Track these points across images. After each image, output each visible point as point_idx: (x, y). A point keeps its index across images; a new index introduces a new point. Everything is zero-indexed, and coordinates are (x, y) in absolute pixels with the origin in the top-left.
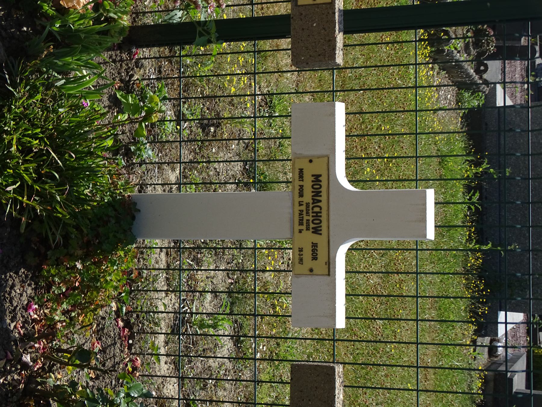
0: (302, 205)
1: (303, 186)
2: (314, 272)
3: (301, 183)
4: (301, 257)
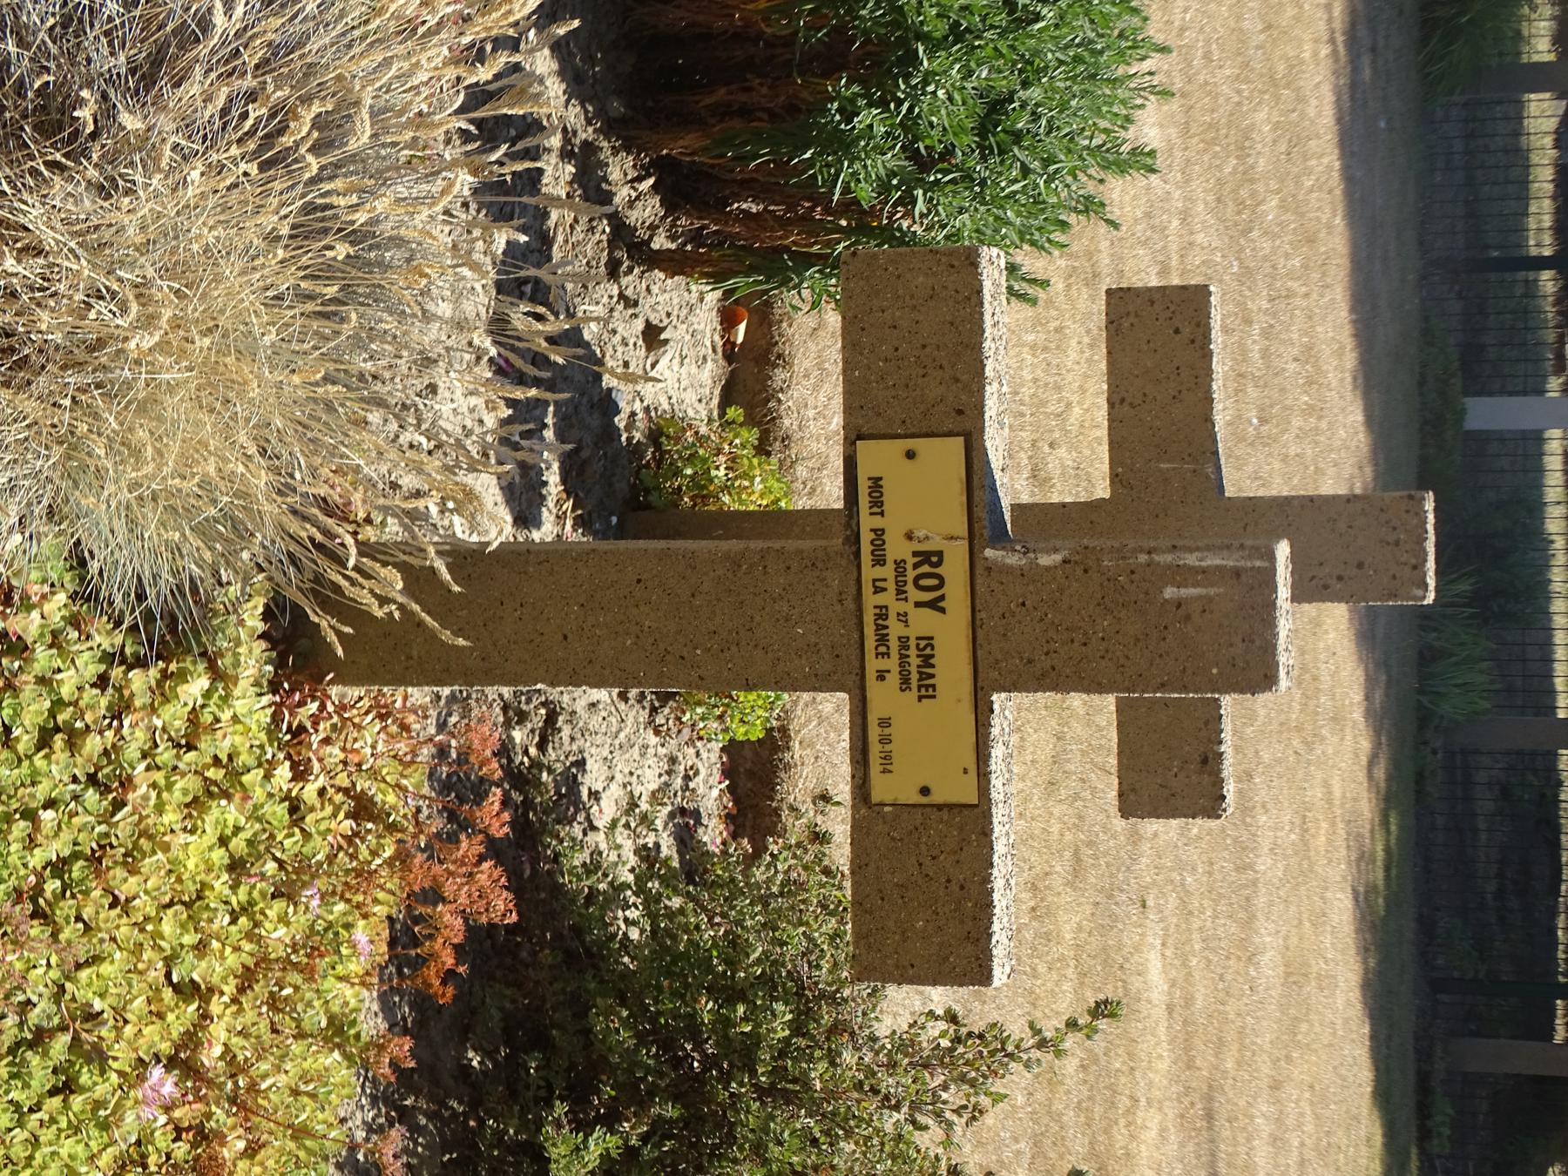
3: (877, 522)
4: (888, 747)
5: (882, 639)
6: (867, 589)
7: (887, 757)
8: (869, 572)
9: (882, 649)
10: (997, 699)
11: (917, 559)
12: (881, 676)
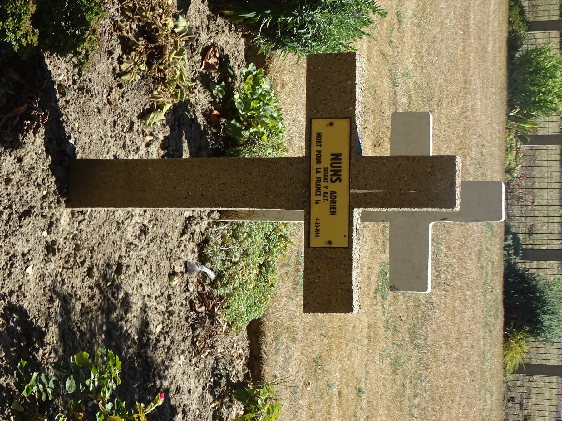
0: (320, 172)
1: (321, 151)
3: (319, 148)
4: (318, 228)
5: (318, 189)
6: (313, 172)
7: (318, 231)
8: (314, 165)
9: (318, 193)
10: (357, 212)
11: (333, 157)
12: (317, 202)
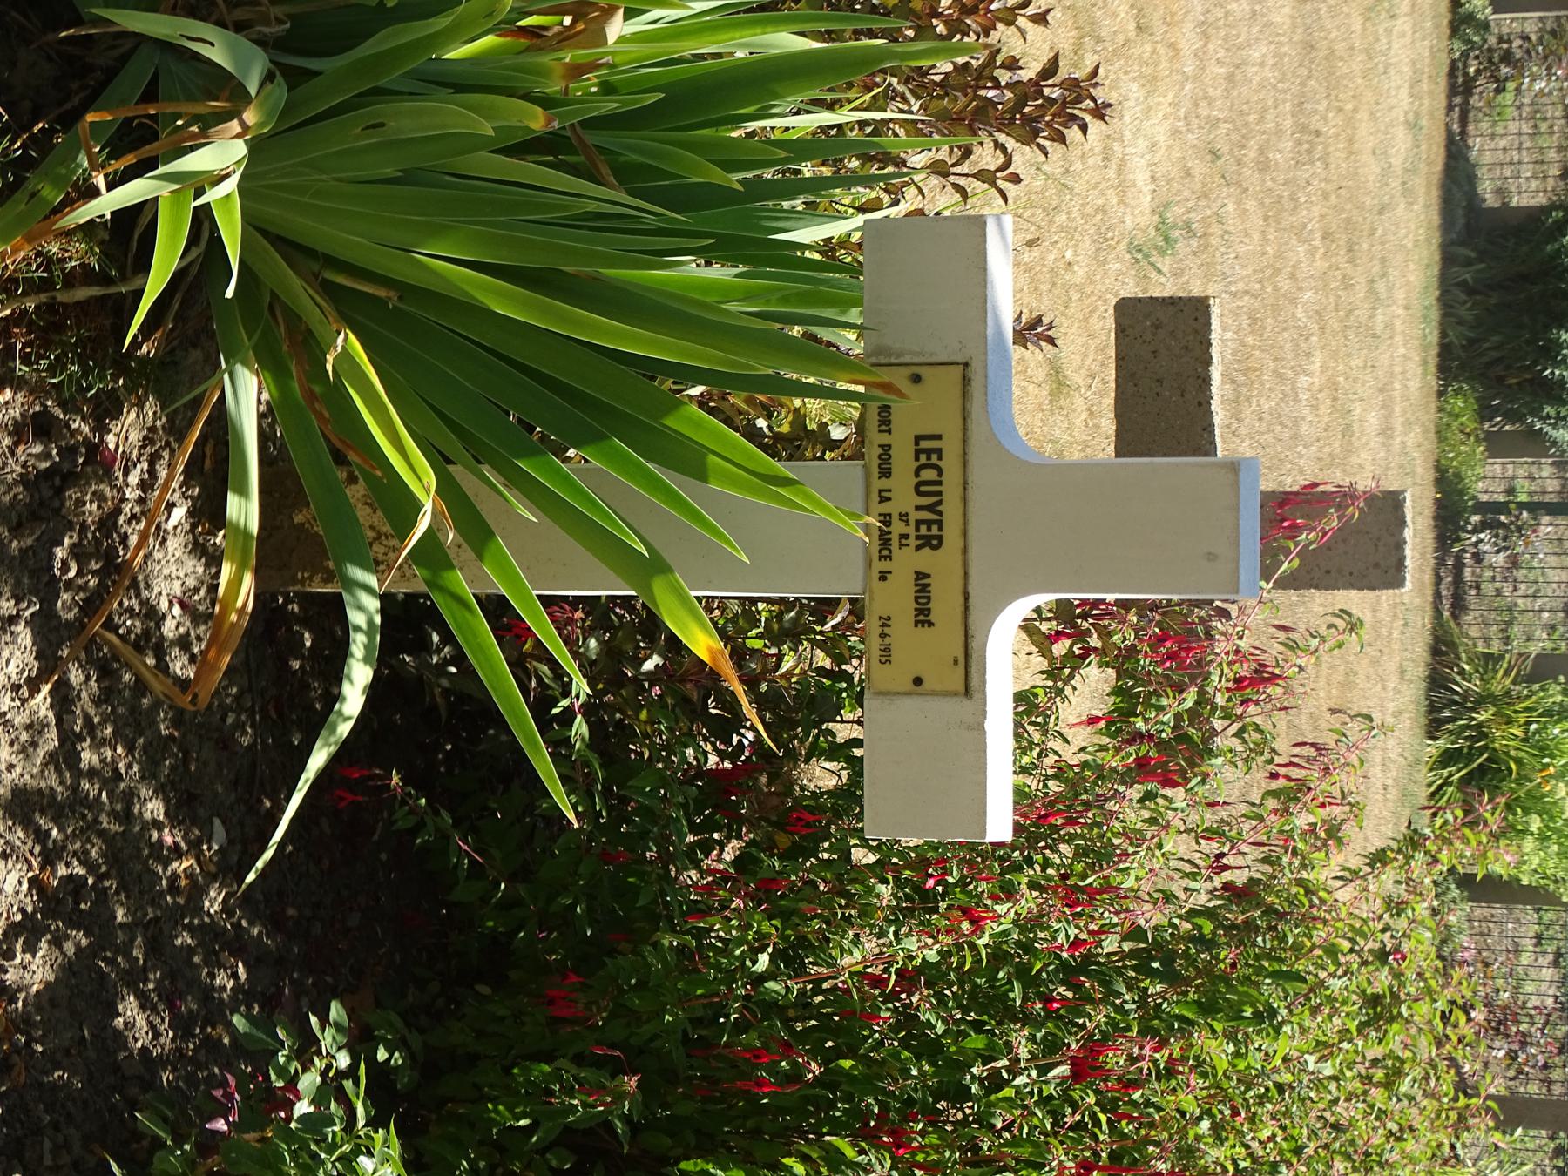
2: (926, 685)
3: (885, 439)
4: (887, 640)
7: (886, 650)
9: (885, 552)
12: (883, 576)
